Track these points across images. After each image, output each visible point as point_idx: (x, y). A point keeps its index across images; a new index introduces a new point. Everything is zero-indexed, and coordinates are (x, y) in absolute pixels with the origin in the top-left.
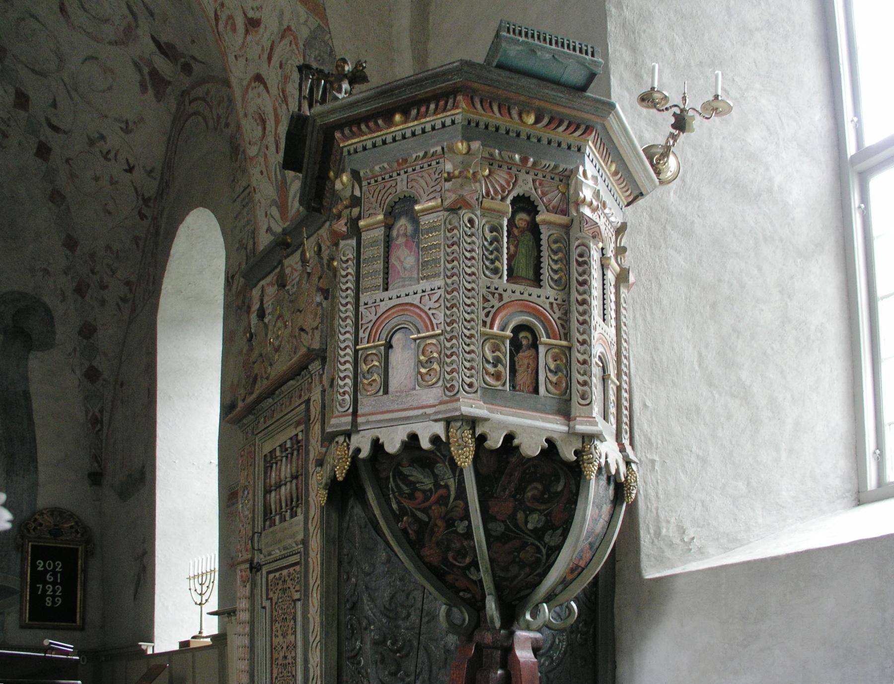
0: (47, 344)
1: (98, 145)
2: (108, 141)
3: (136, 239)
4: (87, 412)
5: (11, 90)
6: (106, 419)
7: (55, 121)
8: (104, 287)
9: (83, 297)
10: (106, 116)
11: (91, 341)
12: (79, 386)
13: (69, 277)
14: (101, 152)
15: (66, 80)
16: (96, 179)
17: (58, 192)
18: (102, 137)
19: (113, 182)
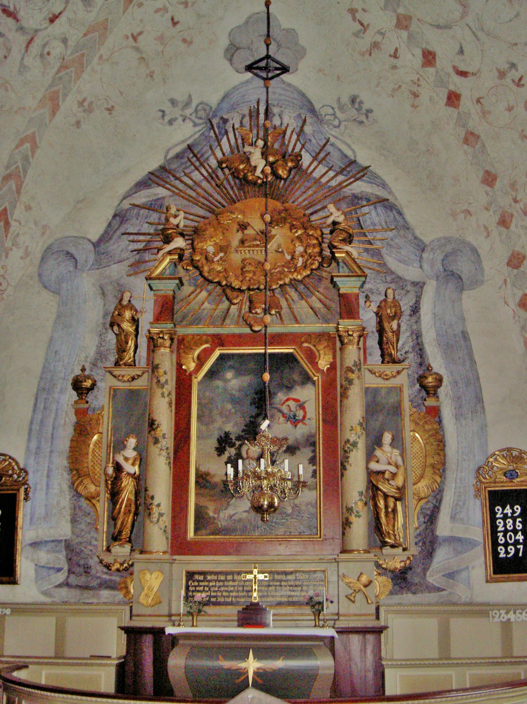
1: (509, 75)
2: (519, 68)
5: (418, 52)
9: (508, 228)
10: (516, 44)
11: (521, 269)
12: (514, 317)
13: (491, 212)
14: (513, 81)
15: (471, 24)
17: (472, 133)
18: (513, 66)
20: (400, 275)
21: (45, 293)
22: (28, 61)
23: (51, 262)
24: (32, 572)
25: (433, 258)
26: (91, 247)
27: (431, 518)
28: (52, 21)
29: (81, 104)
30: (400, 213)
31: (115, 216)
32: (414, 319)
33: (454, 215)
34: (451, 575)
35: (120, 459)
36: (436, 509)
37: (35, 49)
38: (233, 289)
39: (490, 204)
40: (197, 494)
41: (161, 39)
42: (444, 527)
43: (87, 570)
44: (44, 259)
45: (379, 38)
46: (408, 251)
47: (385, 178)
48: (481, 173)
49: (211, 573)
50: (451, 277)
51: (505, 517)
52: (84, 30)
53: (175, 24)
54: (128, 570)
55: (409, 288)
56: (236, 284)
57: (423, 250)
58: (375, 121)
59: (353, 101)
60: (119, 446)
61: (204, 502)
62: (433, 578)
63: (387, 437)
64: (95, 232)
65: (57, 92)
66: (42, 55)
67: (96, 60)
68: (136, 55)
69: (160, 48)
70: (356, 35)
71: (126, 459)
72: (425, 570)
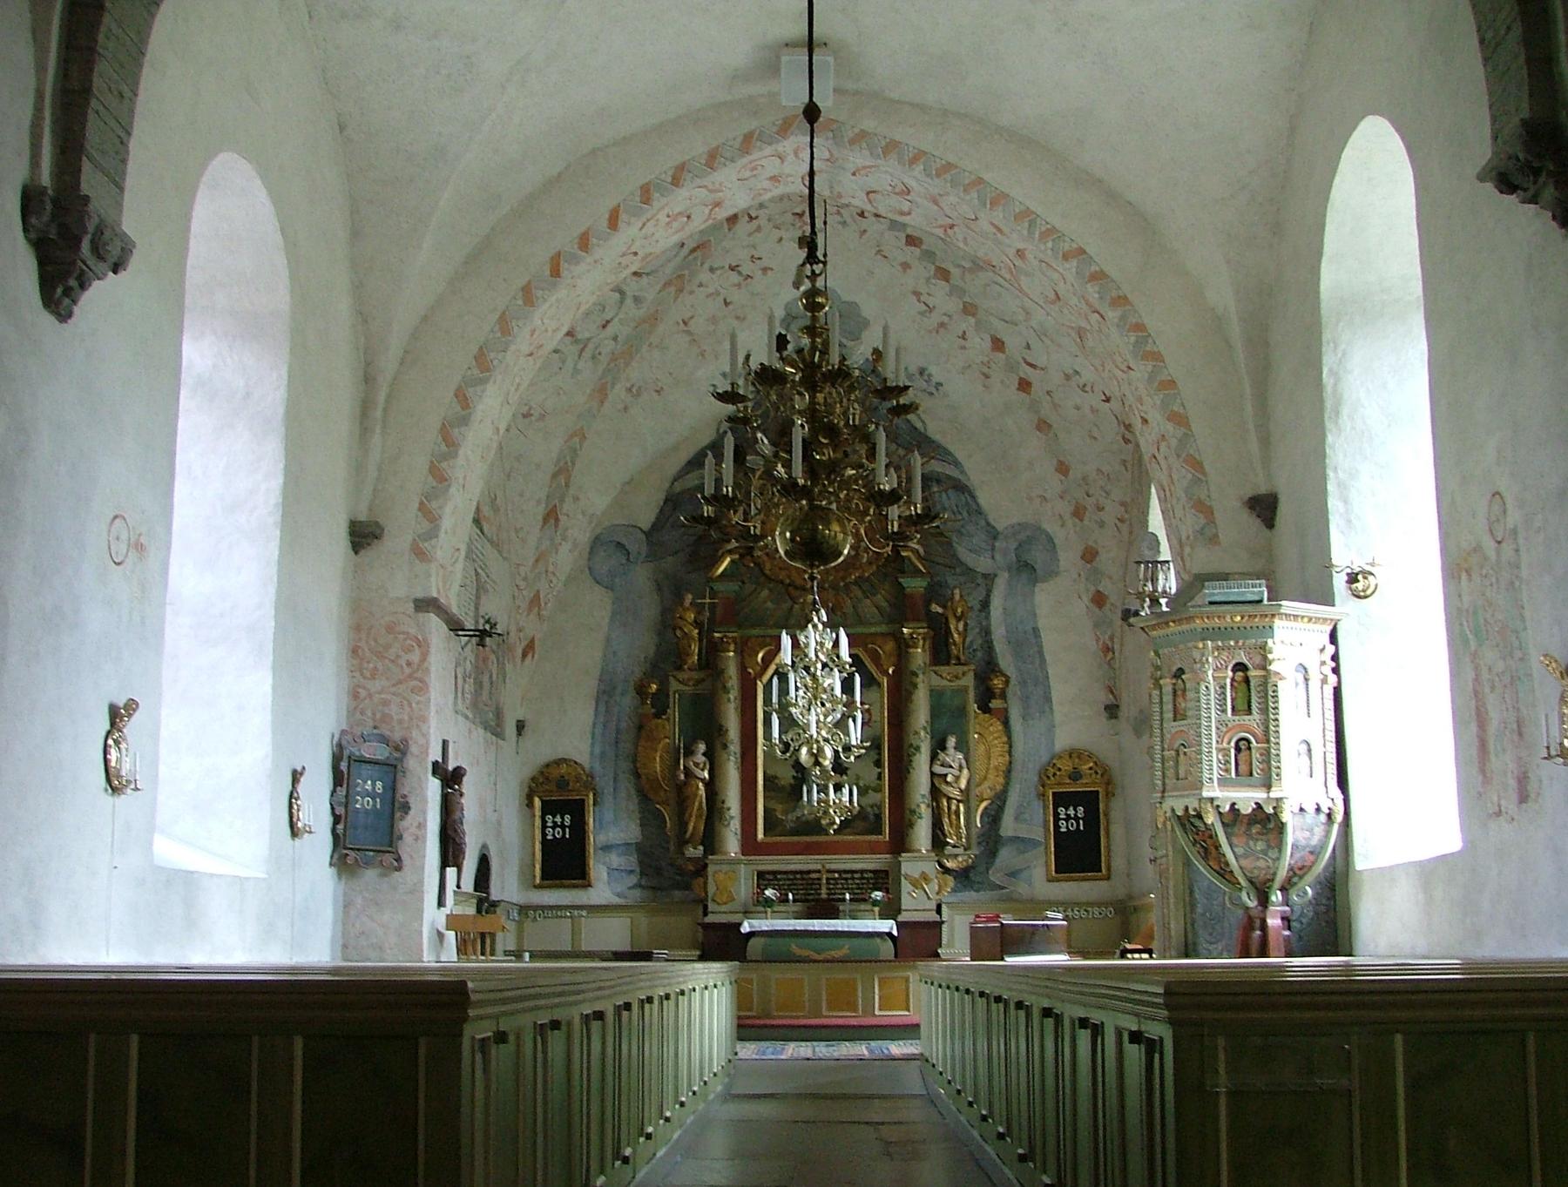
0: (1052, 573)
3: (1124, 462)
6: (1117, 647)
7: (1029, 360)
8: (1101, 509)
19: (1094, 410)
20: (971, 565)
21: (597, 588)
22: (581, 365)
26: (643, 537)
27: (994, 817)
29: (629, 390)
30: (973, 497)
33: (1030, 499)
34: (1013, 874)
36: (1001, 809)
37: (588, 353)
39: (1064, 492)
40: (765, 797)
41: (714, 320)
42: (1008, 827)
44: (592, 551)
45: (946, 319)
46: (979, 539)
48: (1055, 462)
49: (781, 873)
51: (1068, 818)
52: (633, 324)
53: (726, 304)
54: (701, 869)
55: (980, 581)
56: (799, 582)
57: (995, 538)
58: (946, 395)
59: (922, 372)
60: (689, 752)
62: (995, 876)
64: (646, 519)
66: (593, 357)
67: (645, 348)
68: (688, 338)
69: (712, 328)
70: (922, 313)
71: (697, 765)
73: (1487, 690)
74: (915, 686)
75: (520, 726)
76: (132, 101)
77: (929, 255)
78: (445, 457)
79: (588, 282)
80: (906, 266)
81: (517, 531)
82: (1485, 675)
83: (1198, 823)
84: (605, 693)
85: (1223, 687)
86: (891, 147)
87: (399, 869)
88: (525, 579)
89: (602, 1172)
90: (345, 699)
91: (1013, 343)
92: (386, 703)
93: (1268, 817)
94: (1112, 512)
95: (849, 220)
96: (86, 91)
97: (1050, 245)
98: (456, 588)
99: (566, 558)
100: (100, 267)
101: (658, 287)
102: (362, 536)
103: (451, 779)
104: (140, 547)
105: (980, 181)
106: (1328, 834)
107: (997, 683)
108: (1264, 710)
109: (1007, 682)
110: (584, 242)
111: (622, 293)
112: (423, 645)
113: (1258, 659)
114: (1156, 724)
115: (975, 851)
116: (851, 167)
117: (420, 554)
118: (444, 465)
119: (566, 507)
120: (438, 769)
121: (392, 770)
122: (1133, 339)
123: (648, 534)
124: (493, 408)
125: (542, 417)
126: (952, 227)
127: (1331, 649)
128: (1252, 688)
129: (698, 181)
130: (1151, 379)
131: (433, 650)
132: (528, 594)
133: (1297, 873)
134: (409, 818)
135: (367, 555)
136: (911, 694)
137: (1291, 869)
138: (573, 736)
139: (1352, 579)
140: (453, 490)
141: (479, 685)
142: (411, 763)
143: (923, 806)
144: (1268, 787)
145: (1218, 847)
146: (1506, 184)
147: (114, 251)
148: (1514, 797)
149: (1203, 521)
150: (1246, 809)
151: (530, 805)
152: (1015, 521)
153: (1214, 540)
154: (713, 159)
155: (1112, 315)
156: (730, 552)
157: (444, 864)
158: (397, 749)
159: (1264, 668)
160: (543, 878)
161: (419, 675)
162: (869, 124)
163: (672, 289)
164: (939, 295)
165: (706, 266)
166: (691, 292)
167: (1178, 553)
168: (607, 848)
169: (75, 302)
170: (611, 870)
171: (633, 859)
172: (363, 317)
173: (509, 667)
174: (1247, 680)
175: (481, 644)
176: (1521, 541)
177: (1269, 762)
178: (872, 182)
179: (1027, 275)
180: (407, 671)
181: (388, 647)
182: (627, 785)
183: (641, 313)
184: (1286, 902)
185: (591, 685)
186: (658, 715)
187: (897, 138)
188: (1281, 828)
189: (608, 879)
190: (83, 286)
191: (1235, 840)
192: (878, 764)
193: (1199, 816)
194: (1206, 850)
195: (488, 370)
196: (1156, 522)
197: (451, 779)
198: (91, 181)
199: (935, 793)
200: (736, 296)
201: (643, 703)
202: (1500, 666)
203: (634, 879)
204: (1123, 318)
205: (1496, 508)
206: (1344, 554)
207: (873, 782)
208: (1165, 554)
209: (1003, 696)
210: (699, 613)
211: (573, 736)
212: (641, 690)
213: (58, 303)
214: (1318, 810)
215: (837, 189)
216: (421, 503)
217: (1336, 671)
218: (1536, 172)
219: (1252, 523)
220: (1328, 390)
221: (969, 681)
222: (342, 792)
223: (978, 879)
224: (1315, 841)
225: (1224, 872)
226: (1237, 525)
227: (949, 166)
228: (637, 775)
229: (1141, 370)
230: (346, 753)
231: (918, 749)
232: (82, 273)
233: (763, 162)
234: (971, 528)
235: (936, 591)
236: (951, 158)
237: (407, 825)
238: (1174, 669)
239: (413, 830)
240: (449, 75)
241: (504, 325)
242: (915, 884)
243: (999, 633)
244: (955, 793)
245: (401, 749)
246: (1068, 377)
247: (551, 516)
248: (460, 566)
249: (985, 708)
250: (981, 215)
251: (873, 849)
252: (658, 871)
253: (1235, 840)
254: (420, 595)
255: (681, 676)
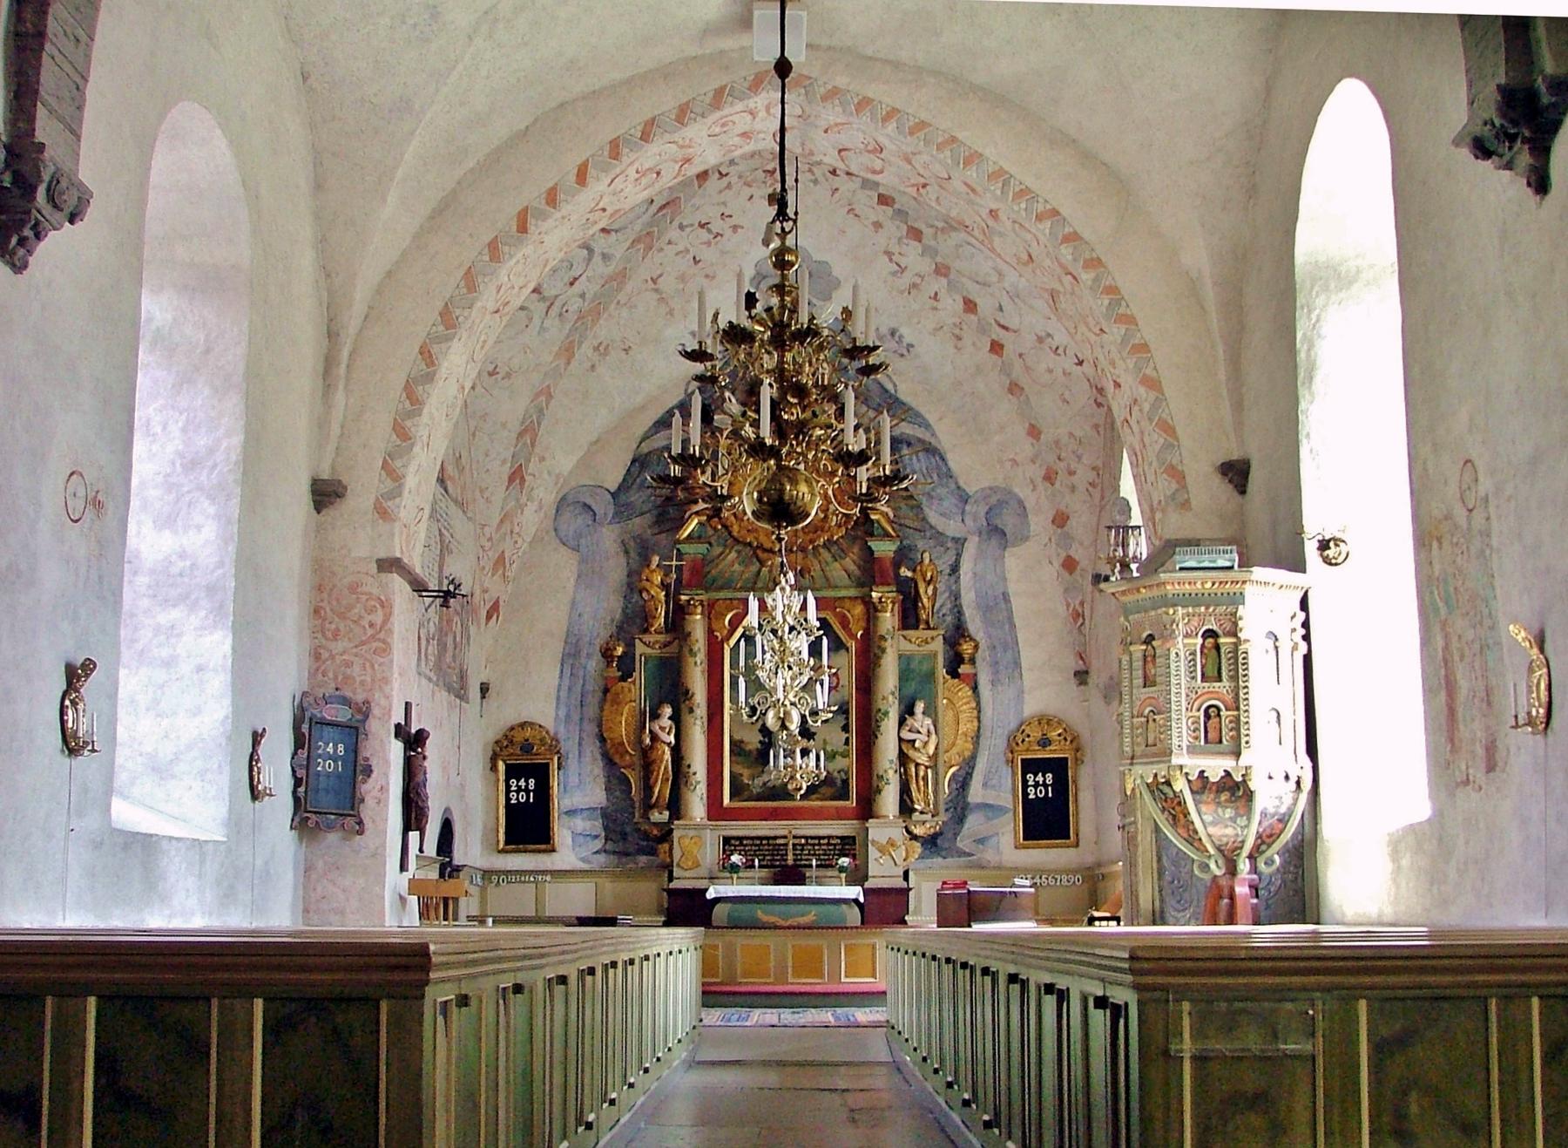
0: (1026, 539)
3: (1096, 426)
4: (1068, 605)
6: (1087, 613)
8: (1072, 473)
16: (1050, 371)
18: (1049, 335)
21: (563, 549)
23: (567, 515)
24: (569, 841)
25: (977, 510)
27: (962, 783)
28: (572, 284)
29: (596, 349)
31: (633, 462)
32: (953, 579)
33: (1000, 462)
34: (981, 841)
35: (656, 728)
36: (969, 775)
38: (765, 550)
41: (682, 278)
42: (976, 793)
43: (624, 836)
45: (918, 281)
46: (950, 503)
47: (927, 416)
50: (995, 533)
51: (1036, 785)
53: (696, 261)
55: (949, 545)
56: (767, 545)
58: (917, 356)
59: (893, 334)
60: (655, 716)
61: (739, 769)
62: (963, 843)
63: (920, 707)
64: (613, 480)
65: (572, 342)
67: (613, 306)
68: (657, 296)
70: (894, 274)
72: (956, 835)
73: (1456, 658)
74: (883, 651)
75: (484, 689)
76: (89, 47)
77: (901, 214)
78: (410, 415)
79: (556, 237)
80: (878, 225)
81: (481, 491)
82: (1455, 644)
83: (1166, 789)
84: (571, 654)
85: (1193, 653)
86: (864, 103)
87: (361, 832)
88: (490, 539)
89: (565, 1137)
90: (307, 662)
91: (985, 304)
92: (349, 664)
93: (1237, 785)
94: (1083, 476)
95: (821, 179)
96: (41, 35)
97: (1023, 206)
98: (419, 549)
99: (531, 519)
100: (56, 217)
101: (628, 244)
102: (325, 494)
103: (414, 741)
104: (97, 505)
105: (954, 139)
106: (1296, 800)
107: (967, 648)
108: (1234, 678)
109: (976, 647)
110: (552, 198)
111: (590, 251)
112: (386, 605)
113: (1228, 626)
114: (1125, 690)
115: (943, 817)
116: (823, 124)
117: (383, 513)
118: (408, 423)
119: (532, 467)
120: (400, 731)
121: (353, 733)
122: (1106, 302)
123: (614, 495)
124: (458, 364)
125: (508, 376)
126: (924, 186)
127: (1301, 616)
128: (1221, 656)
129: (667, 137)
130: (1124, 341)
131: (396, 611)
132: (493, 555)
133: (1264, 841)
134: (371, 780)
135: (329, 514)
136: (879, 658)
137: (1259, 836)
138: (539, 699)
139: (1324, 545)
140: (416, 449)
141: (442, 647)
142: (373, 725)
143: (891, 772)
144: (1237, 754)
145: (1186, 814)
146: (1482, 149)
147: (70, 200)
148: (1481, 765)
149: (1174, 486)
150: (1215, 776)
151: (494, 768)
152: (987, 485)
153: (1186, 505)
154: (683, 114)
155: (1086, 277)
156: (697, 513)
157: (407, 828)
158: (359, 711)
159: (1235, 635)
160: (507, 843)
161: (382, 636)
162: (841, 81)
163: (642, 246)
164: (913, 257)
165: (676, 223)
166: (661, 250)
167: (1150, 513)
168: (571, 813)
169: (30, 252)
170: (575, 835)
171: (599, 824)
172: (326, 271)
173: (473, 630)
174: (1217, 647)
175: (445, 605)
176: (1492, 509)
177: (1238, 730)
178: (844, 139)
179: (1001, 235)
180: (370, 632)
181: (350, 608)
182: (592, 749)
183: (611, 269)
184: (1254, 870)
185: (557, 647)
186: (623, 679)
187: (871, 95)
188: (1249, 796)
189: (574, 840)
190: (38, 237)
191: (1204, 808)
192: (846, 728)
193: (1168, 783)
194: (1174, 817)
195: (454, 327)
196: (1127, 488)
197: (414, 741)
198: (46, 129)
199: (903, 758)
200: (707, 255)
201: (609, 664)
202: (1470, 634)
203: (598, 844)
204: (1096, 280)
205: (1467, 477)
206: (1315, 522)
207: (842, 748)
208: (1136, 519)
209: (972, 661)
210: (666, 575)
211: (539, 699)
212: (607, 654)
213: (13, 253)
214: (1287, 778)
215: (809, 146)
216: (385, 465)
217: (1307, 638)
218: (1512, 139)
219: (1222, 489)
220: (1302, 356)
221: (938, 646)
222: (303, 754)
223: (946, 845)
224: (1283, 810)
225: (1192, 838)
226: (1208, 490)
227: (922, 125)
228: (603, 740)
229: (1116, 332)
230: (308, 715)
231: (886, 714)
232: (37, 223)
233: (735, 118)
234: (941, 491)
235: (903, 555)
236: (924, 116)
237: (369, 788)
238: (1145, 635)
239: (375, 793)
240: (415, 25)
241: (470, 282)
242: (882, 850)
243: (968, 599)
244: (923, 759)
245: (364, 710)
246: (1040, 340)
247: (517, 476)
248: (423, 526)
249: (954, 673)
250: (955, 175)
251: (840, 815)
252: (624, 836)
253: (1204, 808)
254: (383, 555)
255: (647, 638)
